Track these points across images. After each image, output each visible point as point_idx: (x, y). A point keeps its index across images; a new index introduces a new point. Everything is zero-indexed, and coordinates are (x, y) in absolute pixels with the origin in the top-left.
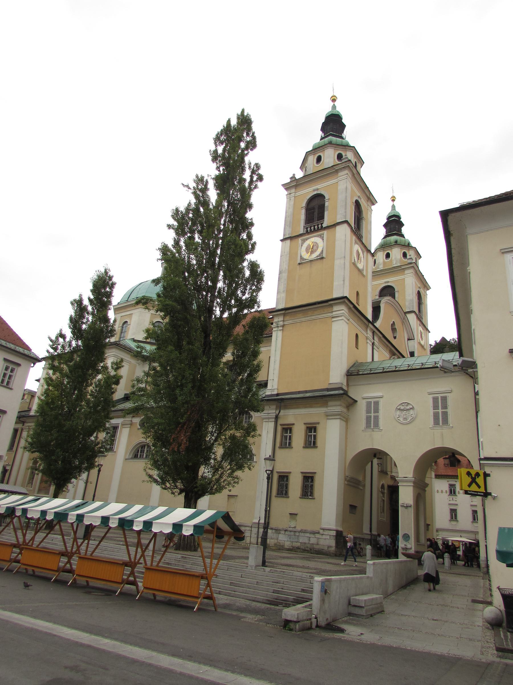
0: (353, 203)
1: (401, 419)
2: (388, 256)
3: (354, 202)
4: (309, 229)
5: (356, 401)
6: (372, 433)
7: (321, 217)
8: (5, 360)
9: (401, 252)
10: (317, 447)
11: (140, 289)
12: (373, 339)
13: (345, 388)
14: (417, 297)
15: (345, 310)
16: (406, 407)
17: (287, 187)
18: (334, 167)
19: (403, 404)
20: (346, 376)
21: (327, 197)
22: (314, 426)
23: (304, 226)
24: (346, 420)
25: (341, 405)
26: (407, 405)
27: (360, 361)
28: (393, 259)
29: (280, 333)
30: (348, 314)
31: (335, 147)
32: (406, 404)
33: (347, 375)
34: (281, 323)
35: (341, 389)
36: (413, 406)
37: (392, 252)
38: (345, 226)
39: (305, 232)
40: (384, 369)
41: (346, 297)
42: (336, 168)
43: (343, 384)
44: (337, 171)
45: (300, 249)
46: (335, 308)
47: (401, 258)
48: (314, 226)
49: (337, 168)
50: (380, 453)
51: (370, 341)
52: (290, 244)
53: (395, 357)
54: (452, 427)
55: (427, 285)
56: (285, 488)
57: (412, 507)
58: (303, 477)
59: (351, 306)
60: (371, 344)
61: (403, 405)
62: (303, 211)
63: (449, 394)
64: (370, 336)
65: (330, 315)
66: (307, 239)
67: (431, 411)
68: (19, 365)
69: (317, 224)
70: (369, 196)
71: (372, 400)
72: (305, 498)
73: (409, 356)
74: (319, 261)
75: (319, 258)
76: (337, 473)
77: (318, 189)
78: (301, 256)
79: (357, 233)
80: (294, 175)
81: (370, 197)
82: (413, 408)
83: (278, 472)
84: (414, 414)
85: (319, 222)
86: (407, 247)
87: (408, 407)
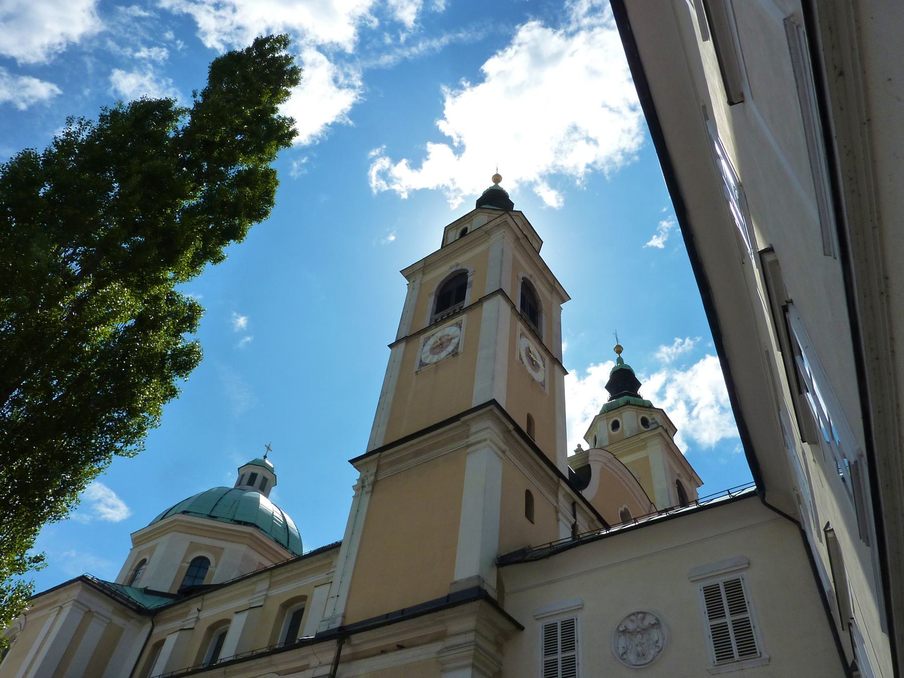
1: (632, 657)
2: (615, 425)
5: (520, 628)
7: (461, 295)
9: (637, 417)
12: (575, 516)
14: (676, 490)
15: (492, 427)
19: (633, 617)
20: (495, 568)
21: (470, 270)
25: (476, 630)
26: (643, 618)
31: (490, 213)
32: (640, 615)
36: (657, 619)
37: (622, 419)
38: (499, 298)
43: (484, 581)
44: (488, 233)
46: (474, 429)
47: (639, 426)
51: (568, 519)
54: (769, 660)
55: (694, 475)
59: (511, 427)
61: (632, 621)
63: (744, 574)
66: (433, 335)
67: (705, 625)
70: (553, 284)
71: (558, 620)
77: (458, 265)
78: (421, 361)
81: (555, 285)
82: (657, 624)
84: (664, 639)
86: (647, 409)
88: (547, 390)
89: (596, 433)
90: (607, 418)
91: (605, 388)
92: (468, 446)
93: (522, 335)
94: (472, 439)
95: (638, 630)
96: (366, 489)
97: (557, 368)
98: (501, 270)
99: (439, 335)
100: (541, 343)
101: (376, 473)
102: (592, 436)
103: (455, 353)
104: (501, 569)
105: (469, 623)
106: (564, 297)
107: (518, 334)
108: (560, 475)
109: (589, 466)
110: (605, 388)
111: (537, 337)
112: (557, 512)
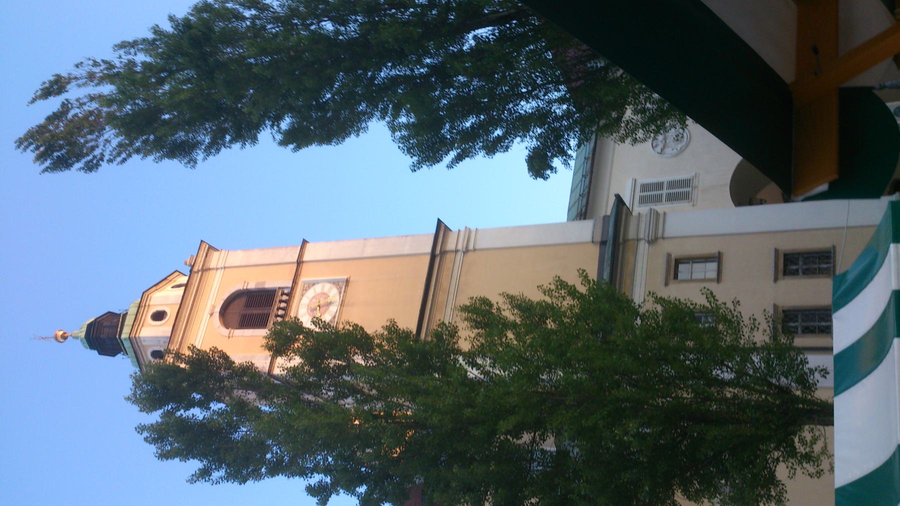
18: (196, 269)
22: (673, 264)
42: (199, 266)
62: (239, 332)
74: (350, 289)
75: (345, 287)
95: (664, 142)
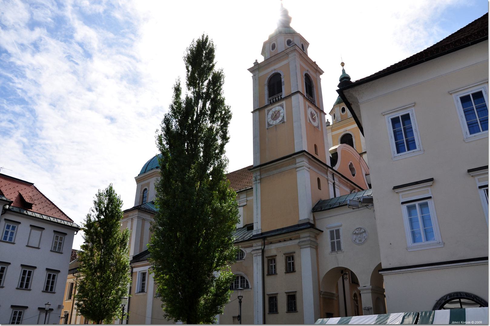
0: (303, 76)
1: (357, 241)
3: (304, 76)
4: (272, 101)
6: (337, 255)
8: (54, 231)
10: (295, 271)
11: (153, 161)
12: (334, 179)
13: (312, 222)
16: (360, 231)
17: (251, 70)
19: (357, 229)
20: (312, 213)
23: (268, 99)
24: (315, 246)
25: (310, 236)
26: (361, 230)
27: (323, 199)
28: (348, 112)
29: (259, 186)
30: (308, 164)
32: (360, 229)
33: (313, 212)
34: (259, 177)
35: (309, 223)
36: (365, 230)
38: (299, 95)
39: (269, 104)
40: (340, 204)
41: (304, 151)
43: (310, 220)
44: (287, 54)
45: (267, 117)
48: (276, 98)
49: (288, 51)
50: (346, 269)
52: (259, 114)
53: (355, 191)
56: (275, 306)
57: (373, 309)
58: (287, 296)
59: (311, 157)
60: (332, 184)
61: (357, 230)
62: (266, 88)
64: (331, 179)
65: (294, 166)
66: (271, 109)
68: (66, 234)
69: (277, 96)
71: (334, 229)
72: (290, 312)
73: (369, 188)
76: (312, 289)
77: (275, 70)
79: (310, 98)
80: (256, 60)
82: (365, 232)
83: (268, 295)
85: (279, 95)
87: (361, 231)
88: (320, 129)
89: (334, 113)
90: (339, 106)
91: (338, 86)
92: (297, 168)
93: (309, 107)
94: (298, 165)
96: (258, 181)
97: (322, 114)
98: (297, 77)
99: (274, 110)
100: (315, 106)
101: (260, 175)
102: (333, 113)
103: (283, 121)
104: (314, 213)
105: (307, 234)
106: (320, 72)
107: (307, 106)
108: (328, 167)
109: (337, 153)
110: (338, 86)
111: (313, 102)
112: (328, 181)
